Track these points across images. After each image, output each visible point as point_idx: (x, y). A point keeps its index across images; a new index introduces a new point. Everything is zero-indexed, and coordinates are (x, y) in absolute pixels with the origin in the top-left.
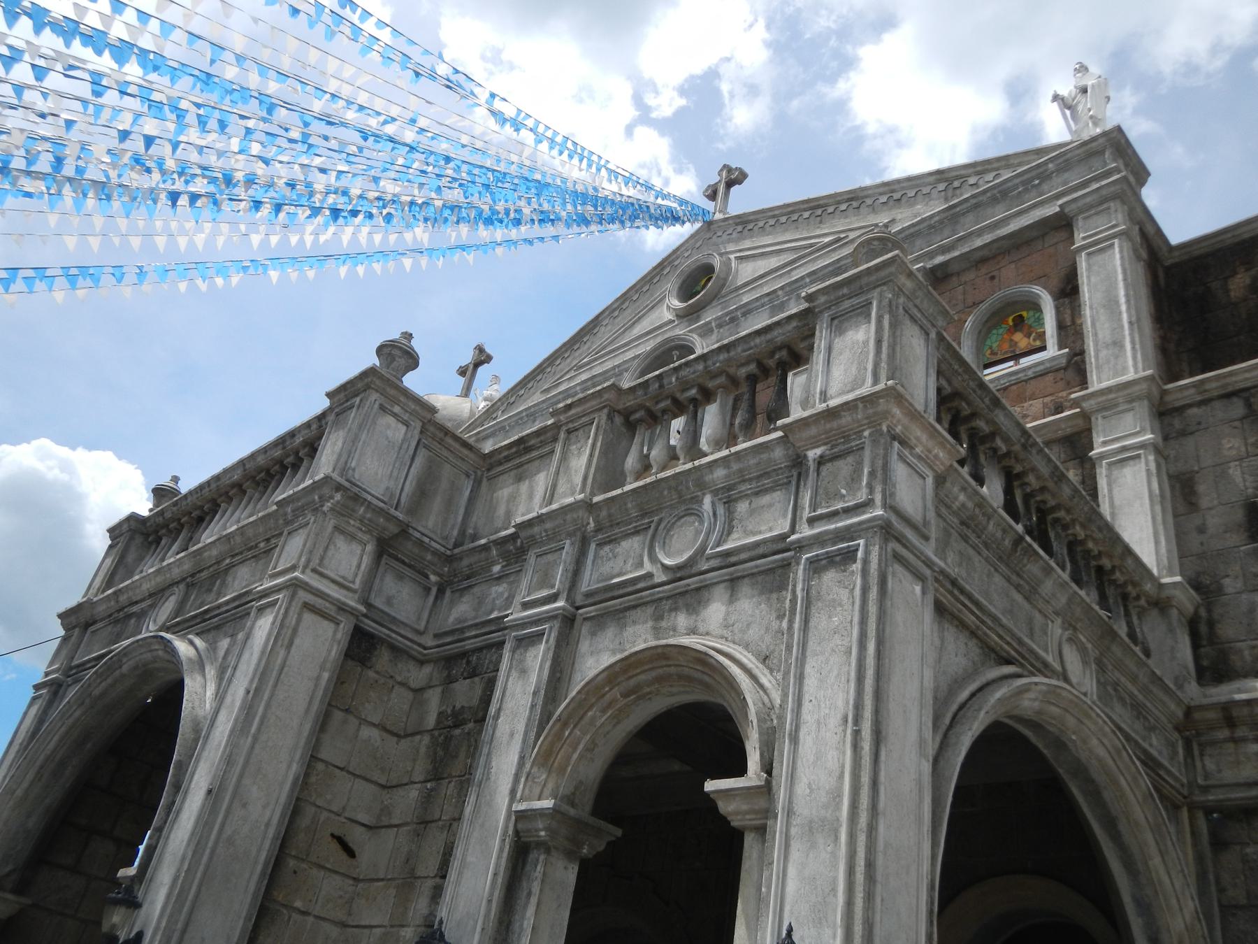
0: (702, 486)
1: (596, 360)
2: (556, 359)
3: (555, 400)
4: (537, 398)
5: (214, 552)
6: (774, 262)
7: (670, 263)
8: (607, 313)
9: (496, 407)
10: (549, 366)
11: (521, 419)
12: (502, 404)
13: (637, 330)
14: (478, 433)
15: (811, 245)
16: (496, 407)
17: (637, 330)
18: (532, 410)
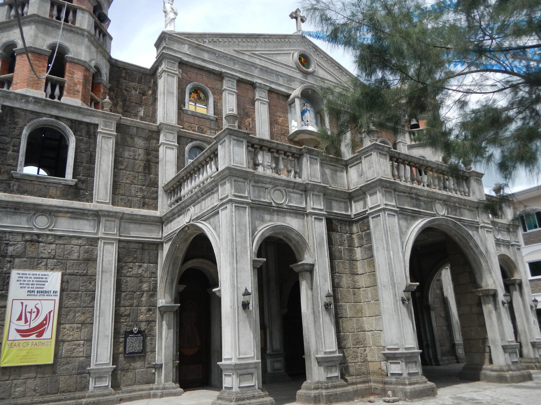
0: (497, 225)
1: (262, 57)
2: (239, 38)
3: (247, 62)
4: (229, 51)
5: (455, 200)
6: (335, 81)
7: (288, 38)
8: (263, 37)
9: (206, 36)
10: (235, 38)
11: (227, 57)
12: (209, 37)
13: (279, 58)
14: (200, 45)
15: (340, 82)
16: (206, 36)
17: (279, 58)
18: (234, 58)
